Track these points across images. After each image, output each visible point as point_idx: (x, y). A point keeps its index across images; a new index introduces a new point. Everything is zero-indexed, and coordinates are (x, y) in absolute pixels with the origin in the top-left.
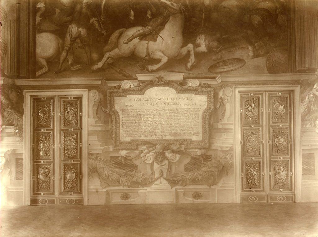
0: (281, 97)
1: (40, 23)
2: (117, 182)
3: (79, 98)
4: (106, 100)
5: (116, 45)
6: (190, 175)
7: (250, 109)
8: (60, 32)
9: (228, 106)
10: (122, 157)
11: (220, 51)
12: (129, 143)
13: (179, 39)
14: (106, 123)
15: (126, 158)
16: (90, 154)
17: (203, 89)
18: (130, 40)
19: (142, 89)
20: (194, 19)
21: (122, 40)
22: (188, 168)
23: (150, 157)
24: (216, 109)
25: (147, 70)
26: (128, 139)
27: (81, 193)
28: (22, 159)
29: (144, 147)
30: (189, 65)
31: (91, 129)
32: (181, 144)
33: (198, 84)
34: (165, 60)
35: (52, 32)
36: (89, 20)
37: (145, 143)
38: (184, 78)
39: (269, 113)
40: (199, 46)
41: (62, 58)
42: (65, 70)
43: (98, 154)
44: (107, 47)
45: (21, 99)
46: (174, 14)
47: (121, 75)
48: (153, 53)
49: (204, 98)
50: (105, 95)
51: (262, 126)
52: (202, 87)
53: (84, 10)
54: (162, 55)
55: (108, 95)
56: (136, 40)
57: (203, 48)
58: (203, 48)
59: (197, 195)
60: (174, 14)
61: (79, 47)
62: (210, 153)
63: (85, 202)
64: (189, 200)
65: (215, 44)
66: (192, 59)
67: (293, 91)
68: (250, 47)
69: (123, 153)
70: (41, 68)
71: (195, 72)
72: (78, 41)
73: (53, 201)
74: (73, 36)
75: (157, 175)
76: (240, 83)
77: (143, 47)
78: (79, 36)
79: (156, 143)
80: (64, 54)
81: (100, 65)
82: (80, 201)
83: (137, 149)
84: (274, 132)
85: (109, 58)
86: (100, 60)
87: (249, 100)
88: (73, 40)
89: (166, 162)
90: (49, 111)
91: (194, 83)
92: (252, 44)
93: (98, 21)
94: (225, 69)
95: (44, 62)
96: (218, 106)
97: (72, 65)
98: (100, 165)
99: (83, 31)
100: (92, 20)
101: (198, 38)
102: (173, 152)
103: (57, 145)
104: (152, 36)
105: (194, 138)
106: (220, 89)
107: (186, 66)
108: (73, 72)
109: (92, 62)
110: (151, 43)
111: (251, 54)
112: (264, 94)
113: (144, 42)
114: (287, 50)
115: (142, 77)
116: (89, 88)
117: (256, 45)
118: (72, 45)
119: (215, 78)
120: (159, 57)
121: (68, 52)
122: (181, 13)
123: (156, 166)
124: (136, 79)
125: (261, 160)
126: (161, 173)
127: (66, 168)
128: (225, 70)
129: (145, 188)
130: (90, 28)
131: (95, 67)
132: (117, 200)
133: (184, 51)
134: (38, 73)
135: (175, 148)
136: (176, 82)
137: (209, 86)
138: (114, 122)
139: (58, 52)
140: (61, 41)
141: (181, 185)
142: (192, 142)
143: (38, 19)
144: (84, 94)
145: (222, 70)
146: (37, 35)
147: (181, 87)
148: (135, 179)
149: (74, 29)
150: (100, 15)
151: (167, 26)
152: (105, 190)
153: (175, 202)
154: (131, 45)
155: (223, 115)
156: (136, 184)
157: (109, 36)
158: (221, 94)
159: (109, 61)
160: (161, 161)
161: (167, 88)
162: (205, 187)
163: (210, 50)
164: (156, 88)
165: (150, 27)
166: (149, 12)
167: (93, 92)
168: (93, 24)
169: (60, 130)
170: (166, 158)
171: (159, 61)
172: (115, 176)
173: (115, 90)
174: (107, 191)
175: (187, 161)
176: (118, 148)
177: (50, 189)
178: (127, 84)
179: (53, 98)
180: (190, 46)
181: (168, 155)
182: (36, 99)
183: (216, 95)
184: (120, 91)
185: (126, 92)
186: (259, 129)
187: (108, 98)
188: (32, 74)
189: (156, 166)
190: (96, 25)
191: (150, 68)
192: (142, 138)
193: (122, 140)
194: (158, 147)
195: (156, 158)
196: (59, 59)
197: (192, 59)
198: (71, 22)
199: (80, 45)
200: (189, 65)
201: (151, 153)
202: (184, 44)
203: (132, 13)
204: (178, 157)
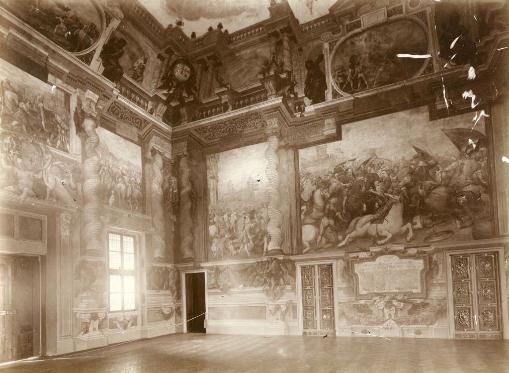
0: (486, 257)
1: (304, 220)
2: (359, 322)
3: (331, 265)
4: (348, 266)
5: (354, 229)
6: (412, 318)
7: (459, 267)
8: (317, 224)
9: (441, 266)
10: (361, 305)
11: (433, 226)
12: (366, 295)
13: (400, 220)
14: (349, 281)
15: (364, 306)
16: (340, 303)
17: (421, 255)
18: (363, 225)
19: (373, 258)
20: (411, 205)
21: (358, 225)
22: (410, 312)
23: (382, 304)
24: (431, 269)
25: (377, 244)
26: (365, 292)
27: (334, 328)
28: (296, 306)
29: (377, 298)
30: (408, 238)
31: (340, 286)
32: (404, 295)
33: (416, 252)
34: (390, 236)
35: (312, 224)
36: (335, 213)
37: (377, 295)
38: (405, 248)
39: (476, 270)
40: (415, 224)
41: (318, 241)
42: (320, 248)
43: (344, 303)
44: (348, 231)
45: (294, 268)
46: (395, 203)
47: (358, 249)
48: (381, 232)
49: (422, 261)
50: (348, 263)
51: (471, 280)
52: (419, 254)
53: (332, 208)
54: (387, 232)
55: (350, 263)
56: (368, 224)
57: (419, 225)
58: (419, 225)
59: (418, 332)
60: (395, 203)
61: (330, 232)
62: (428, 301)
63: (337, 334)
64: (412, 335)
65: (429, 221)
66: (411, 234)
67: (498, 252)
68: (457, 221)
69: (362, 302)
70: (305, 248)
71: (414, 243)
72: (329, 228)
73: (316, 334)
74: (325, 225)
75: (387, 317)
76: (450, 249)
77: (373, 229)
78: (329, 225)
79: (385, 294)
80: (320, 237)
81: (344, 243)
82: (334, 334)
83: (372, 299)
84: (481, 285)
85: (349, 238)
86: (344, 239)
87: (458, 261)
88: (325, 228)
89: (393, 308)
90: (311, 275)
91: (413, 251)
92: (459, 219)
93: (341, 214)
94: (438, 239)
95: (307, 244)
96: (432, 267)
97: (325, 244)
98: (345, 310)
99: (332, 222)
100: (337, 214)
101: (414, 218)
102: (399, 301)
103: (318, 297)
104: (380, 220)
105: (414, 291)
106: (434, 254)
107: (406, 239)
108: (327, 249)
109: (338, 242)
110: (380, 225)
111: (459, 226)
112: (471, 257)
113: (374, 225)
114: (491, 220)
115: (373, 249)
116: (337, 259)
117: (462, 219)
118: (324, 231)
119: (429, 246)
120: (385, 235)
121: (322, 236)
122: (401, 202)
123: (385, 310)
124: (369, 251)
125: (471, 307)
126: (390, 315)
127: (324, 312)
128: (438, 240)
129: (379, 326)
130: (336, 219)
131: (340, 245)
132: (359, 334)
133: (404, 228)
134: (304, 251)
135: (400, 298)
136: (399, 251)
137: (425, 252)
138: (355, 282)
139: (316, 239)
140: (317, 230)
141: (406, 325)
142: (413, 294)
143: (303, 217)
144: (334, 263)
145: (435, 240)
146: (303, 227)
147: (403, 255)
148: (371, 320)
149: (325, 221)
150: (342, 209)
151: (391, 212)
152: (350, 327)
153: (401, 336)
154: (365, 227)
155: (437, 273)
156: (372, 323)
157: (349, 223)
158: (434, 257)
159: (350, 240)
160: (390, 308)
161: (392, 256)
162: (425, 326)
163: (425, 226)
164: (384, 256)
165: (378, 214)
166: (377, 204)
167: (340, 261)
168: (337, 217)
169: (319, 287)
170: (394, 305)
171: (385, 237)
172: (356, 318)
173: (354, 260)
174: (352, 328)
175: (410, 307)
176: (358, 298)
177: (314, 326)
178: (362, 255)
179: (313, 266)
180: (409, 225)
181: (395, 303)
182: (303, 268)
183: (430, 259)
184: (358, 259)
185: (362, 260)
186: (468, 283)
187: (350, 265)
188: (300, 252)
189: (385, 310)
190: (340, 217)
191: (379, 242)
192: (375, 291)
193: (361, 293)
194: (387, 298)
195: (386, 306)
196: (317, 242)
197: (411, 234)
198: (323, 217)
199: (330, 231)
200: (408, 238)
201: (382, 302)
202: (404, 223)
203: (365, 206)
204: (402, 304)
